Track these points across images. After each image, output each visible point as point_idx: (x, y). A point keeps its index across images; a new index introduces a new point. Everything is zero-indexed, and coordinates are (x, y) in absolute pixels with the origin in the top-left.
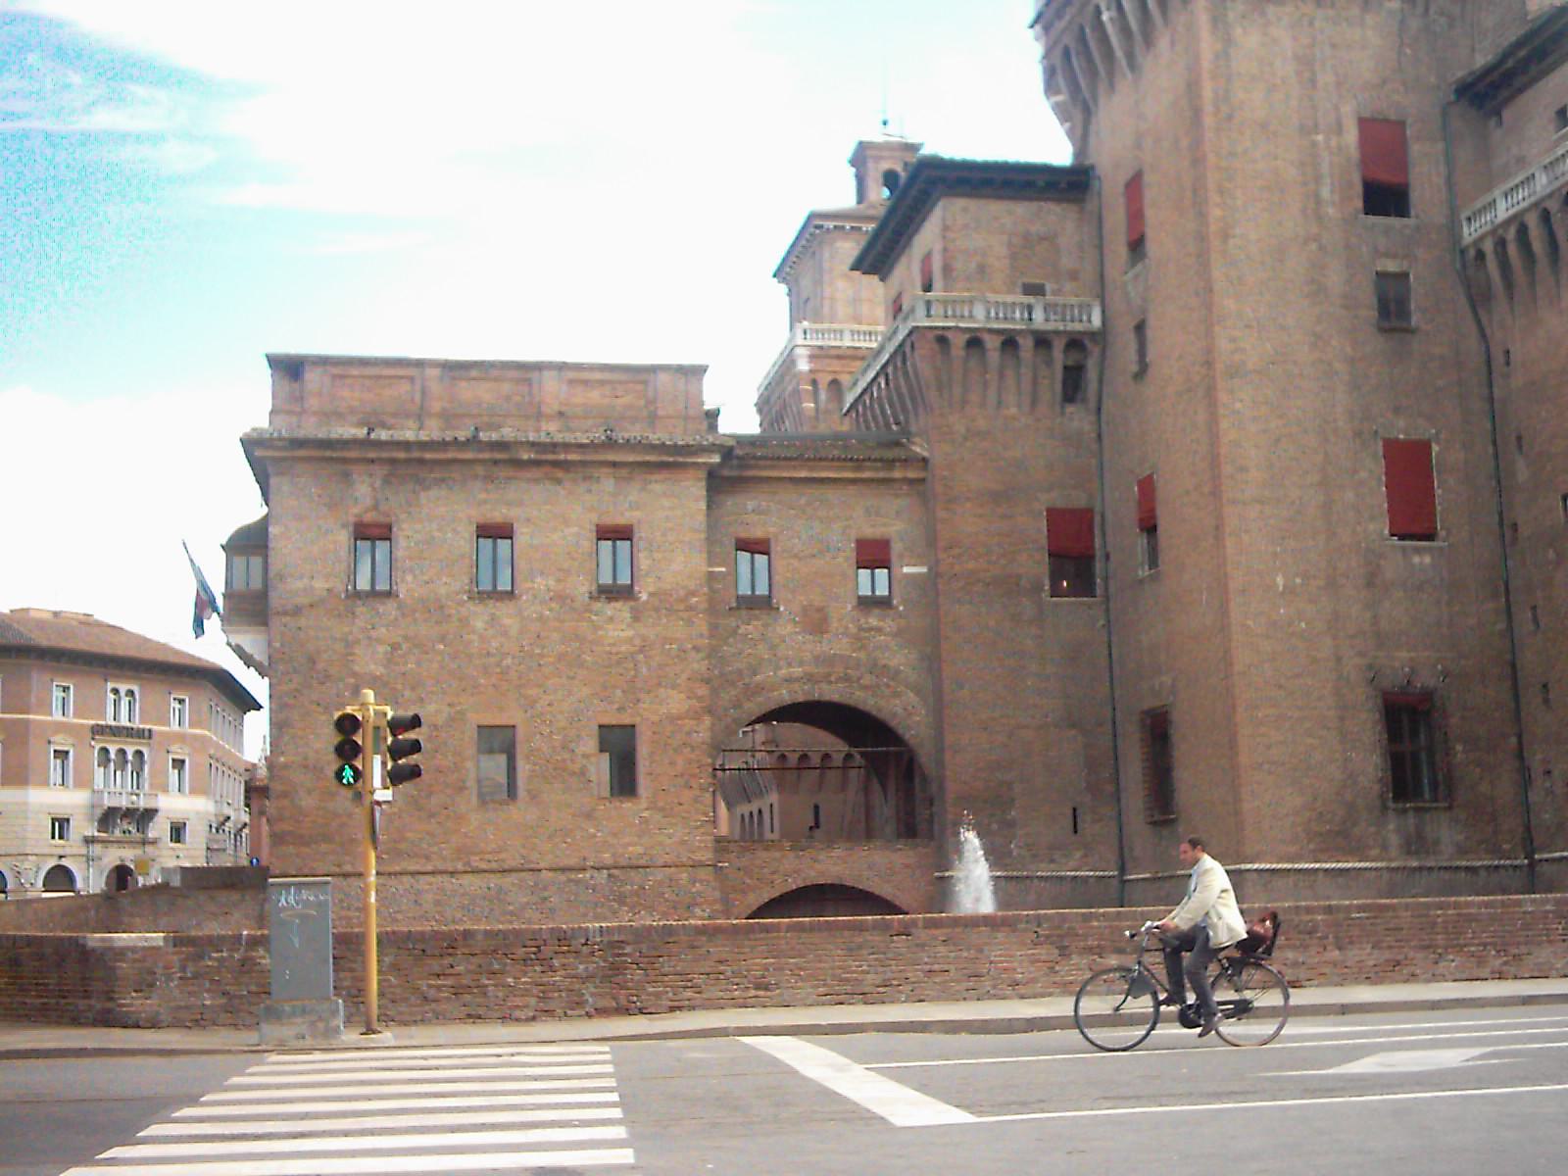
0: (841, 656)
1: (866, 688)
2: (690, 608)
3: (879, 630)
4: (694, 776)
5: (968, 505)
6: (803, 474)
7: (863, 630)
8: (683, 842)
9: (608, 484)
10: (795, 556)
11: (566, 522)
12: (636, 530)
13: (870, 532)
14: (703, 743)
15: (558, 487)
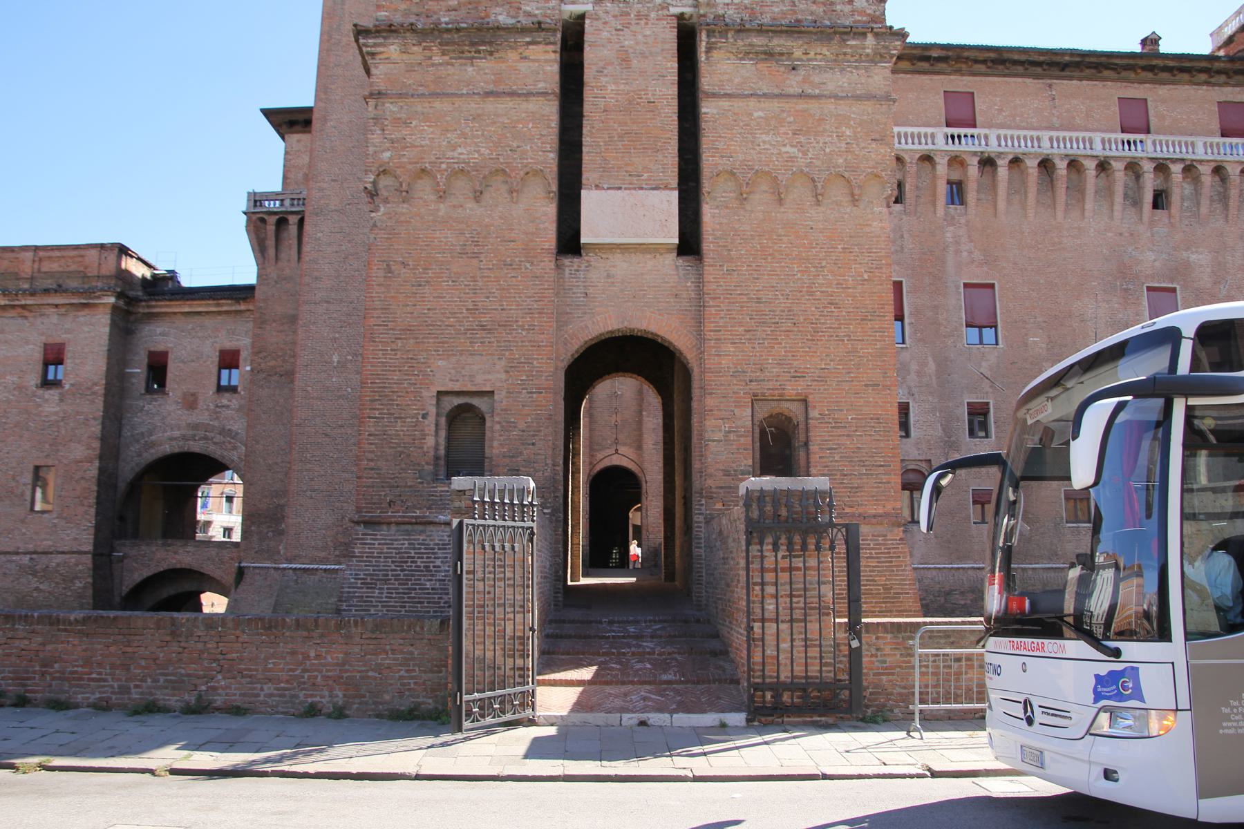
0: (203, 424)
1: (215, 443)
2: (94, 393)
3: (227, 407)
4: (85, 498)
5: (274, 324)
6: (187, 310)
7: (217, 406)
8: (75, 539)
9: (53, 318)
10: (183, 362)
11: (27, 343)
12: (67, 346)
13: (229, 344)
14: (93, 477)
15: (25, 321)
